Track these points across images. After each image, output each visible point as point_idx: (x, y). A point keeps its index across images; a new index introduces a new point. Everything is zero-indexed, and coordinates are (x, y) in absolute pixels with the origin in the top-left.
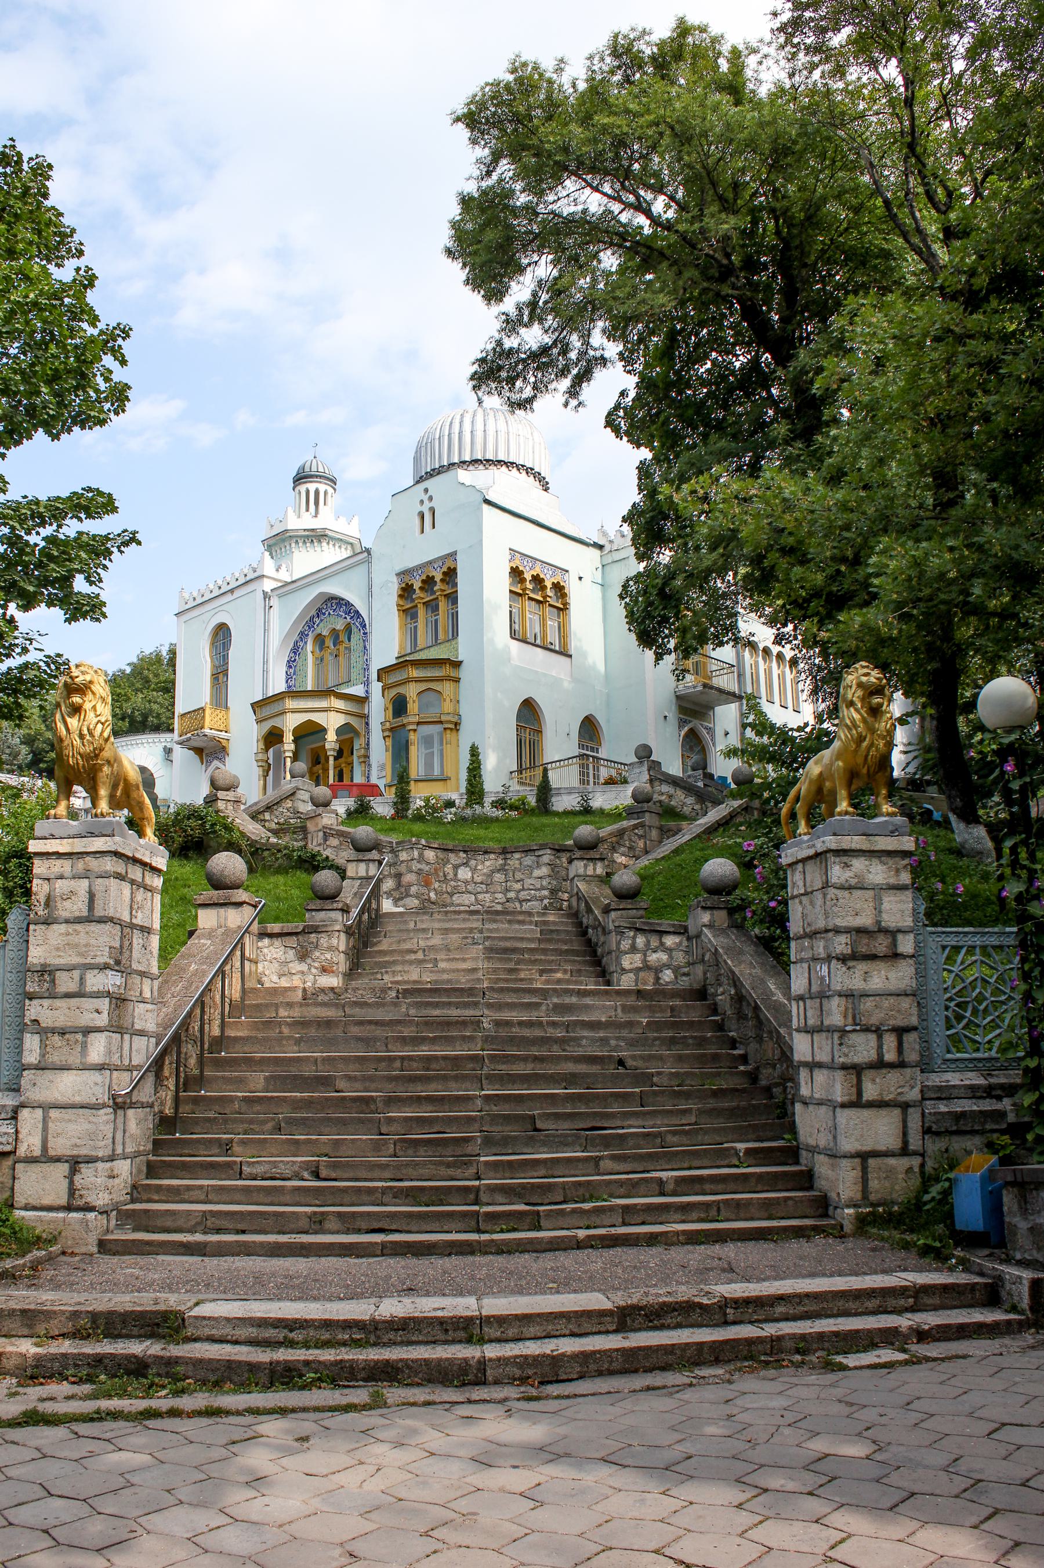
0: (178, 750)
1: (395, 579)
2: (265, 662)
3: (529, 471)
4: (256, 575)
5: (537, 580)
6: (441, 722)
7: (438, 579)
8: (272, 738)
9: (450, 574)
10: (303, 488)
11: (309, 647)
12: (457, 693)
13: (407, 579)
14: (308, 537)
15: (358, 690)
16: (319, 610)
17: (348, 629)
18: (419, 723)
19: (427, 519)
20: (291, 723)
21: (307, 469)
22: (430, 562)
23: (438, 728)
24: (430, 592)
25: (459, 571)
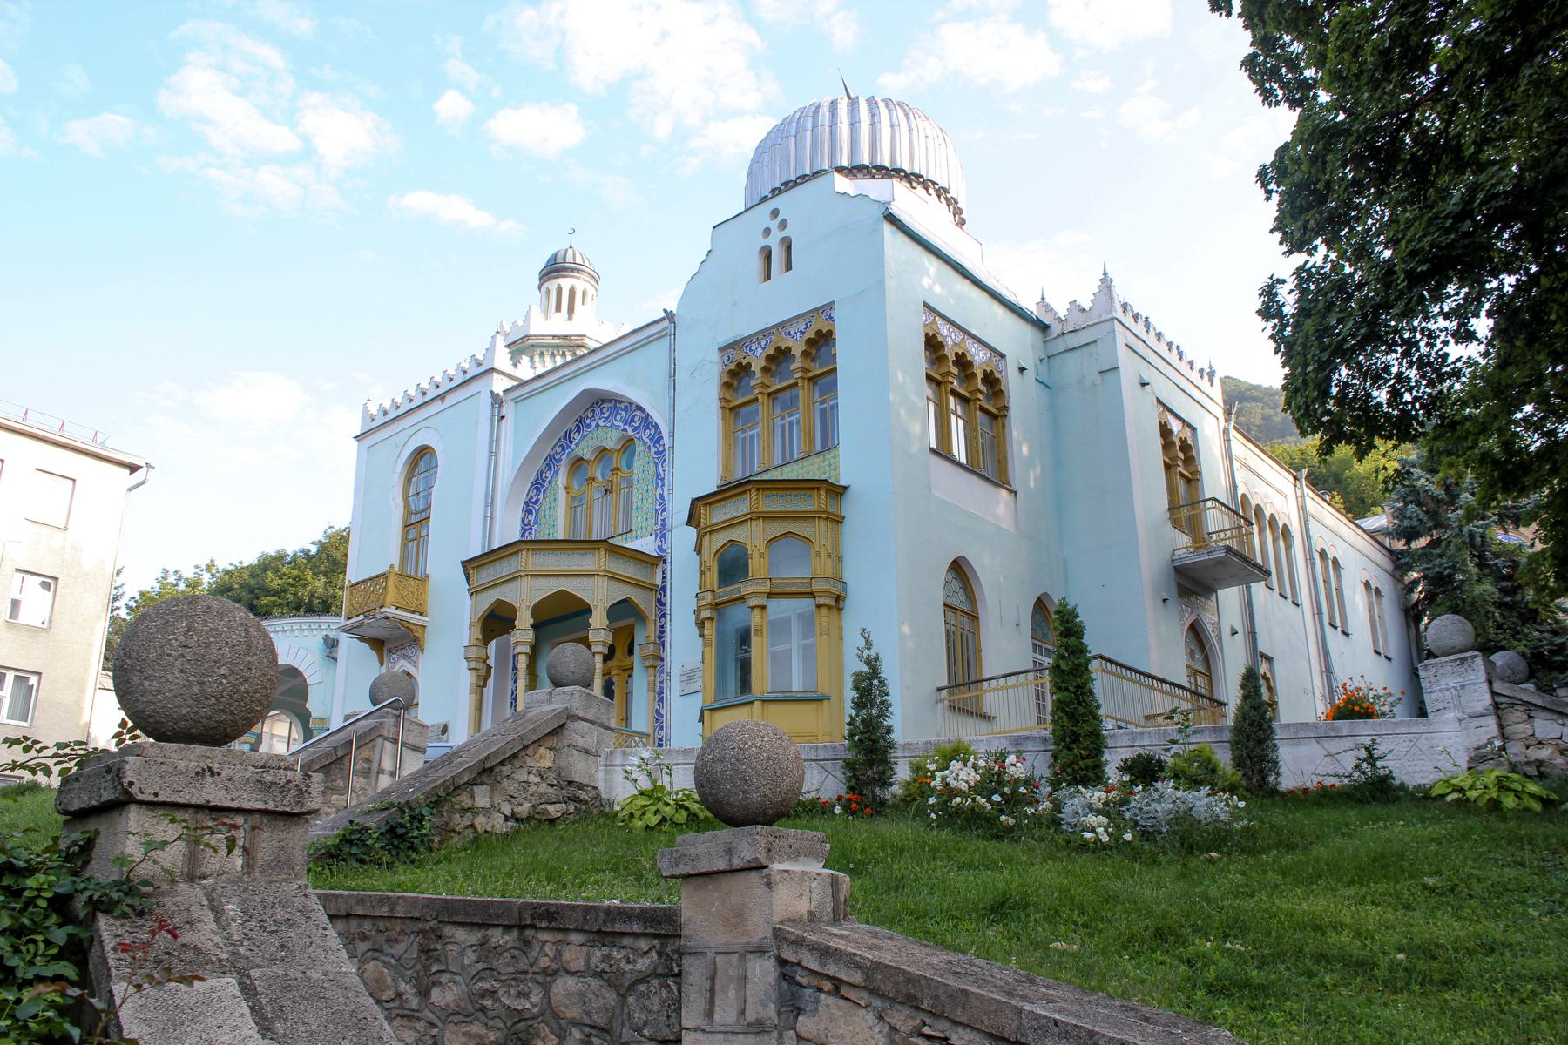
0: (347, 644)
1: (715, 356)
2: (490, 503)
3: (941, 192)
4: (482, 369)
5: (963, 362)
6: (812, 594)
7: (797, 350)
8: (496, 622)
9: (822, 341)
10: (552, 285)
11: (562, 480)
12: (838, 541)
13: (738, 356)
14: (557, 346)
15: (646, 544)
16: (581, 420)
17: (628, 444)
18: (770, 595)
19: (775, 258)
20: (525, 597)
21: (559, 260)
22: (782, 325)
23: (806, 604)
24: (784, 373)
25: (838, 335)
